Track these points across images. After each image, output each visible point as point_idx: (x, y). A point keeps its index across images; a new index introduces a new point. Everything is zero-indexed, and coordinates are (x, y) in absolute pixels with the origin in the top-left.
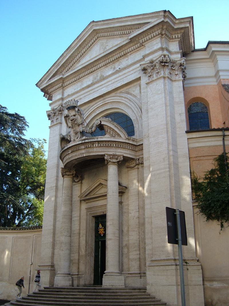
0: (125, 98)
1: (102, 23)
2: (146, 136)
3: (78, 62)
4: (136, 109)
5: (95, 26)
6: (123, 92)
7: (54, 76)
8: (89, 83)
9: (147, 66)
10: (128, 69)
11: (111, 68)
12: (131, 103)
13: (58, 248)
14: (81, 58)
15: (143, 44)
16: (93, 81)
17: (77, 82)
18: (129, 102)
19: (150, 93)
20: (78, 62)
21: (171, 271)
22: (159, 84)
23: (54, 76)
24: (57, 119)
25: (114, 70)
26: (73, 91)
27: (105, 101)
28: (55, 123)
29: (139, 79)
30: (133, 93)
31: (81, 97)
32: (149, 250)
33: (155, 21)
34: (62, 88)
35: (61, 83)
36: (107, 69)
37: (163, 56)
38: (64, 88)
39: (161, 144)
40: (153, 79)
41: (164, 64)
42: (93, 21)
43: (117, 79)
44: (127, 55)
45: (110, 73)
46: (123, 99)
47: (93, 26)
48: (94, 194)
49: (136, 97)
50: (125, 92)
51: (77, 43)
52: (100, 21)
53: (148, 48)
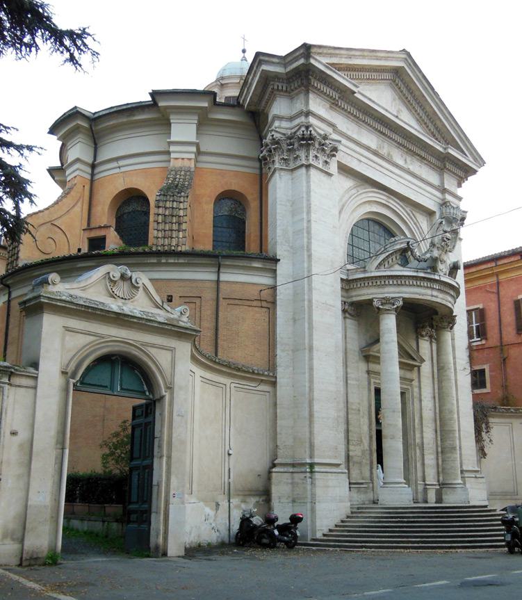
1: (420, 77)
8: (373, 146)
27: (389, 202)
33: (470, 161)
42: (408, 54)
52: (420, 72)
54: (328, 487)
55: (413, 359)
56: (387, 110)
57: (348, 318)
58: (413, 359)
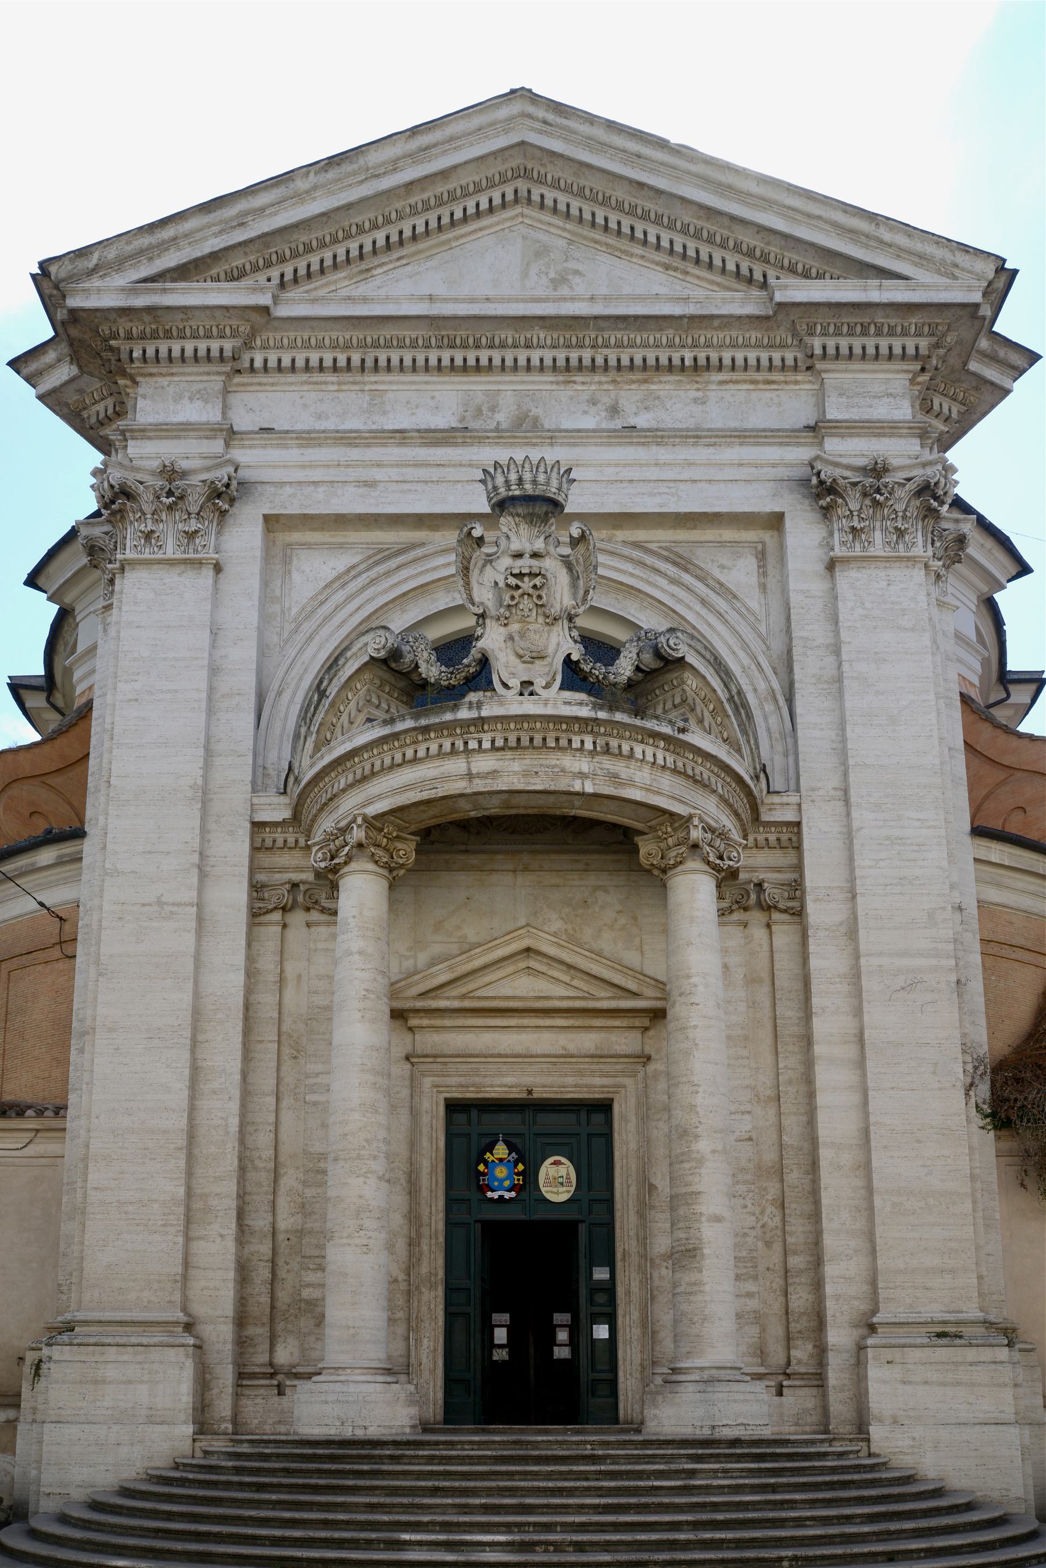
0: (673, 581)
2: (817, 793)
3: (361, 272)
4: (741, 654)
5: (537, 125)
6: (649, 545)
7: (183, 272)
8: (442, 421)
9: (845, 478)
10: (711, 450)
11: (593, 402)
12: (712, 619)
13: (222, 1236)
14: (386, 260)
15: (819, 366)
16: (463, 419)
17: (339, 384)
18: (698, 607)
19: (852, 609)
20: (361, 272)
21: (993, 1366)
22: (903, 586)
23: (183, 272)
24: (191, 535)
25: (612, 418)
26: (305, 422)
28: (171, 550)
29: (776, 521)
30: (717, 573)
31: (378, 474)
32: (842, 1280)
34: (227, 368)
35: (238, 342)
36: (565, 394)
37: (940, 467)
38: (238, 379)
39: (915, 848)
40: (872, 551)
41: (935, 504)
43: (635, 474)
44: (706, 376)
45: (588, 423)
46: (662, 582)
47: (528, 122)
48: (463, 997)
49: (735, 597)
50: (666, 553)
51: (396, 160)
53: (841, 395)
54: (104, 1382)
55: (635, 995)
56: (472, 300)
57: (317, 924)
58: (635, 995)
